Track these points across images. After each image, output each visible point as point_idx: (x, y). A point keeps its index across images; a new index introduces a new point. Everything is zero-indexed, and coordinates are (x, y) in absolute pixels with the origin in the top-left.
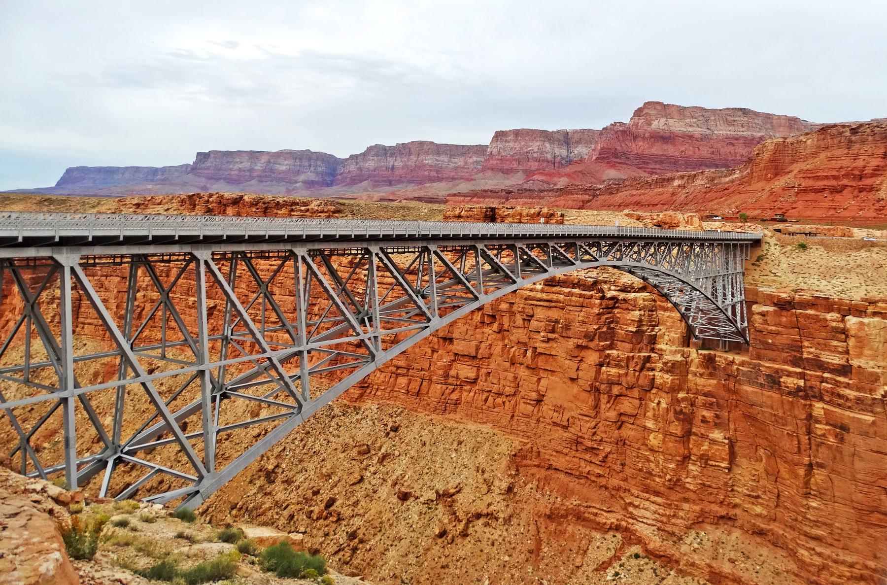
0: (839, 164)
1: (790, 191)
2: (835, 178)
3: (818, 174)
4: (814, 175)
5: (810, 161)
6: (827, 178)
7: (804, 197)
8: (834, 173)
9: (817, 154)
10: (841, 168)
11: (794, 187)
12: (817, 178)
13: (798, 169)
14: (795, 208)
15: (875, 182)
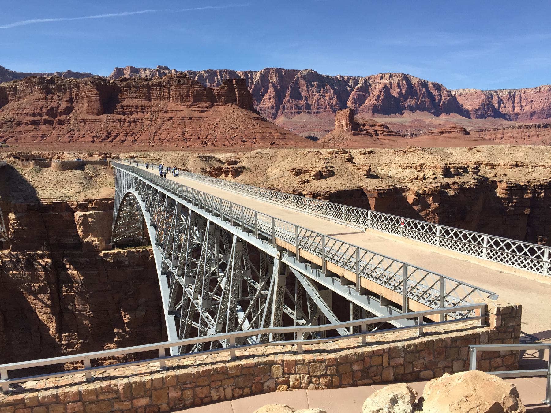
0: (41, 104)
1: (8, 124)
2: (40, 115)
3: (28, 111)
4: (24, 112)
5: (20, 102)
6: (34, 115)
7: (19, 128)
8: (38, 111)
9: (25, 96)
10: (43, 107)
11: (10, 121)
12: (27, 114)
13: (11, 108)
14: (12, 137)
15: (66, 118)
